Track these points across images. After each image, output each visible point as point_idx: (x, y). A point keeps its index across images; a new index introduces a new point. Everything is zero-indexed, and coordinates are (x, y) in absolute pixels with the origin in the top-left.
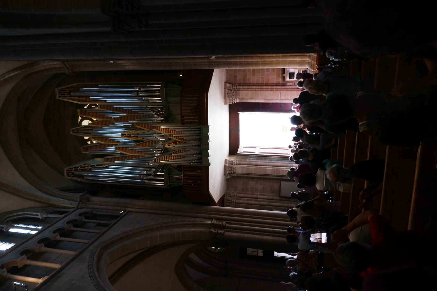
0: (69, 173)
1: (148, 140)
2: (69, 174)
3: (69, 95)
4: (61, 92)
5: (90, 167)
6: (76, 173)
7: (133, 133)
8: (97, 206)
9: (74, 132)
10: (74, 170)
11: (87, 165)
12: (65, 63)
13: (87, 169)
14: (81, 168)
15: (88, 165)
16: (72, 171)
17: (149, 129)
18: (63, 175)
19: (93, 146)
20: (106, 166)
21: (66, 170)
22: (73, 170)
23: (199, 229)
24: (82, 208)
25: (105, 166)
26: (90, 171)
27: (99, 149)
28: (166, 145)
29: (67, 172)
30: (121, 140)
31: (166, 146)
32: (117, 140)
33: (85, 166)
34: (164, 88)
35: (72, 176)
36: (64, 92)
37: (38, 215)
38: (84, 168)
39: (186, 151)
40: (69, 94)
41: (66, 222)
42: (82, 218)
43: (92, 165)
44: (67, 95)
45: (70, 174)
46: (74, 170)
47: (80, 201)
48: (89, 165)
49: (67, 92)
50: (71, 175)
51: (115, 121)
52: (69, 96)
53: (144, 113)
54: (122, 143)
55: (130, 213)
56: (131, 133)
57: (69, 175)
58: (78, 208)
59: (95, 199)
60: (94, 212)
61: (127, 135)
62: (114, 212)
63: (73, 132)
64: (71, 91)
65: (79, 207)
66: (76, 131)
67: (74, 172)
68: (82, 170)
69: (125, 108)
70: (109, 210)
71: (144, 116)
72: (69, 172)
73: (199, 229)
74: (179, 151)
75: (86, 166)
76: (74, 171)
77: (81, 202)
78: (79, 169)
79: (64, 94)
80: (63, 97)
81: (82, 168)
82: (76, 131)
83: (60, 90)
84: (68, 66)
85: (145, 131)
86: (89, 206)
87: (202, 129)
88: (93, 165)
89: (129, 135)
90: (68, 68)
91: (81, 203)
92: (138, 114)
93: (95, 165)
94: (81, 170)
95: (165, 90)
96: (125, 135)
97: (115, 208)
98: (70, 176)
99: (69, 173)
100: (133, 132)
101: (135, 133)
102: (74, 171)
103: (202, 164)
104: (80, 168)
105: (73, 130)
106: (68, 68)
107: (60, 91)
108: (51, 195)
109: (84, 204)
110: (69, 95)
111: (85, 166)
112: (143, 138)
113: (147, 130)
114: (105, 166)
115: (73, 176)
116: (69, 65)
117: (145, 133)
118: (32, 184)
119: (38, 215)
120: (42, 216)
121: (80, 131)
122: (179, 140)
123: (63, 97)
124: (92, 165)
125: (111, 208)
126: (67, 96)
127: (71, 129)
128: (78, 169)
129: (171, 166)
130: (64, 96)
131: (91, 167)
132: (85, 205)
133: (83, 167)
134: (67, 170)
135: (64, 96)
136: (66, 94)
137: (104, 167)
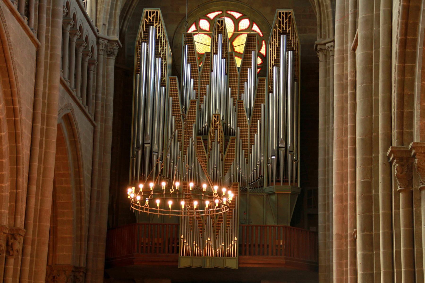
0: (152, 16)
5: (162, 53)
10: (157, 25)
25: (164, 81)
34: (290, 192)
38: (161, 42)
46: (157, 25)
72: (153, 17)
85: (222, 153)
95: (288, 194)
102: (155, 25)
111: (163, 45)
114: (164, 81)
134: (157, 13)
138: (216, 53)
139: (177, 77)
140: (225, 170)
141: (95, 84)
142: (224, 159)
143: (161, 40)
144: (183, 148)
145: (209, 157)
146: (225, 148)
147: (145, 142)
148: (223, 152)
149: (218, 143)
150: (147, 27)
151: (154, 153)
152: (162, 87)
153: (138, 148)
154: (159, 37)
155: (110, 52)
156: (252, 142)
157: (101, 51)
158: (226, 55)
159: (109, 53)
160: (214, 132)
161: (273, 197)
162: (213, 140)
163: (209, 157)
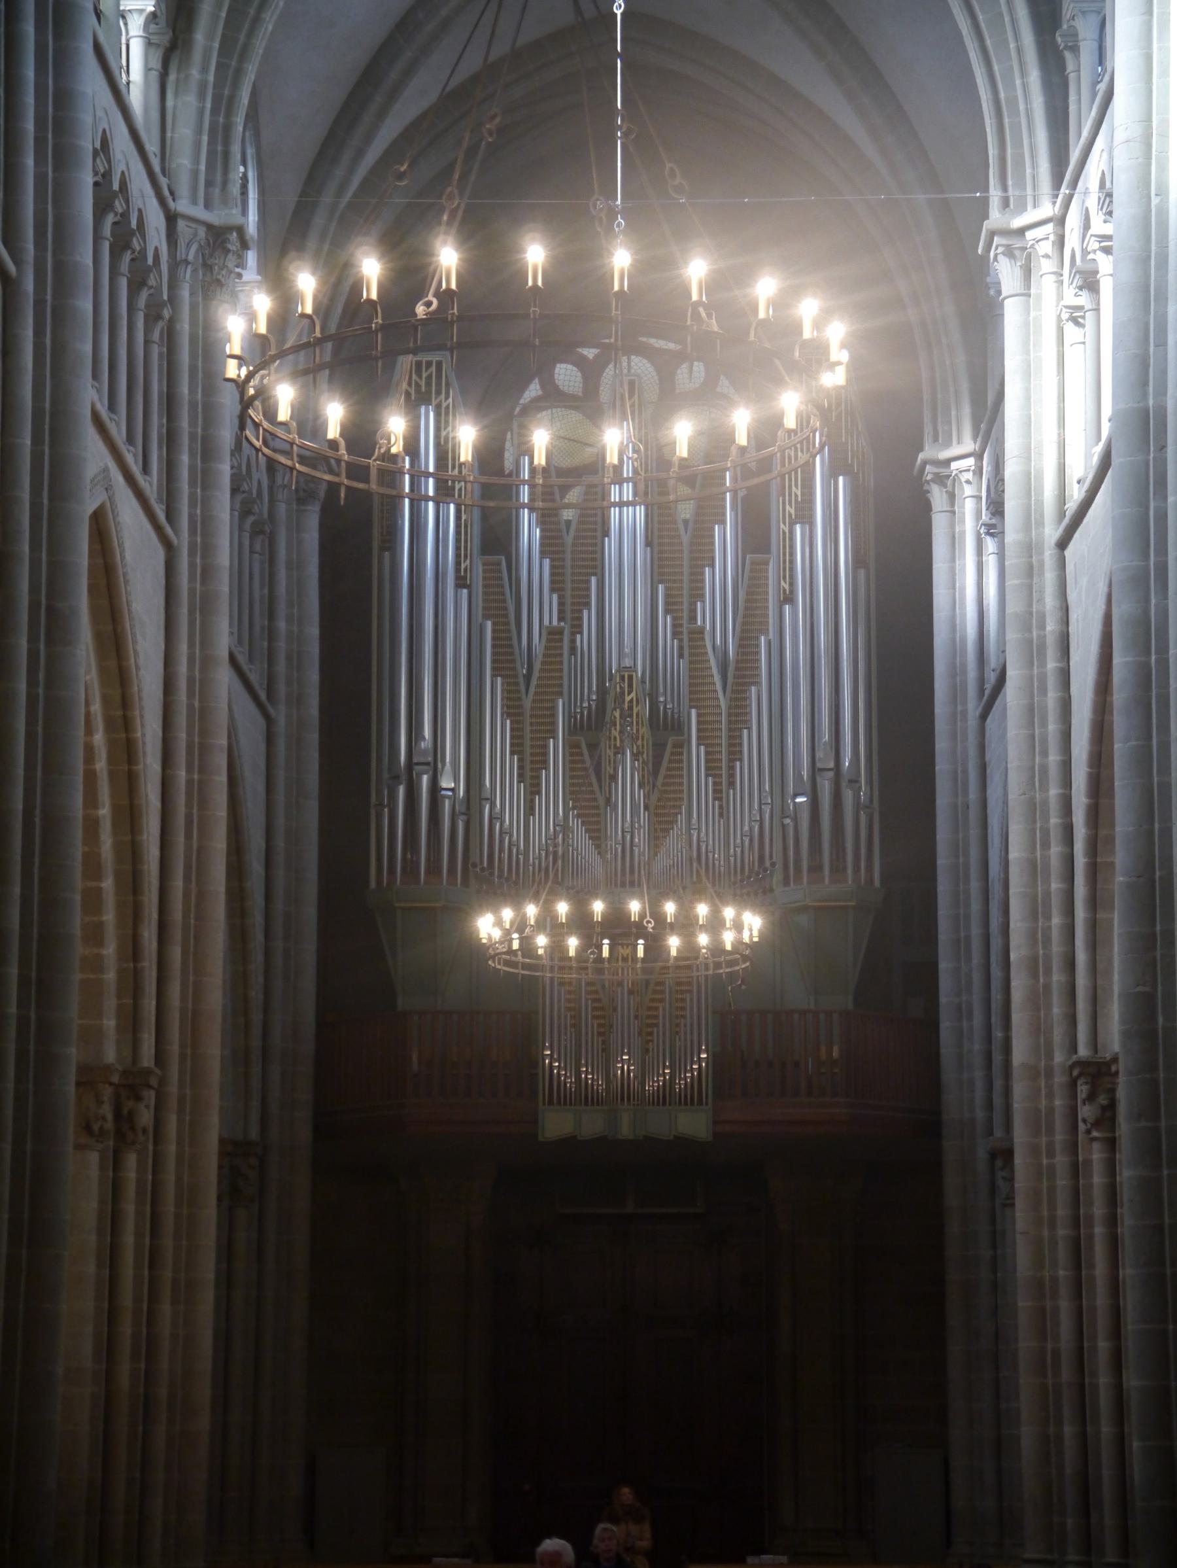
0: (424, 375)
17: (657, 807)
22: (443, 396)
25: (466, 570)
29: (429, 364)
34: (853, 904)
39: (599, 1034)
45: (423, 383)
71: (721, 783)
74: (599, 1000)
85: (647, 788)
86: (282, 508)
89: (631, 708)
92: (730, 753)
97: (282, 645)
100: (644, 729)
112: (614, 778)
125: (282, 625)
134: (439, 365)
139: (503, 558)
141: (266, 591)
147: (415, 760)
148: (648, 783)
151: (443, 792)
152: (459, 590)
153: (396, 778)
155: (305, 491)
156: (735, 753)
157: (281, 490)
159: (302, 494)
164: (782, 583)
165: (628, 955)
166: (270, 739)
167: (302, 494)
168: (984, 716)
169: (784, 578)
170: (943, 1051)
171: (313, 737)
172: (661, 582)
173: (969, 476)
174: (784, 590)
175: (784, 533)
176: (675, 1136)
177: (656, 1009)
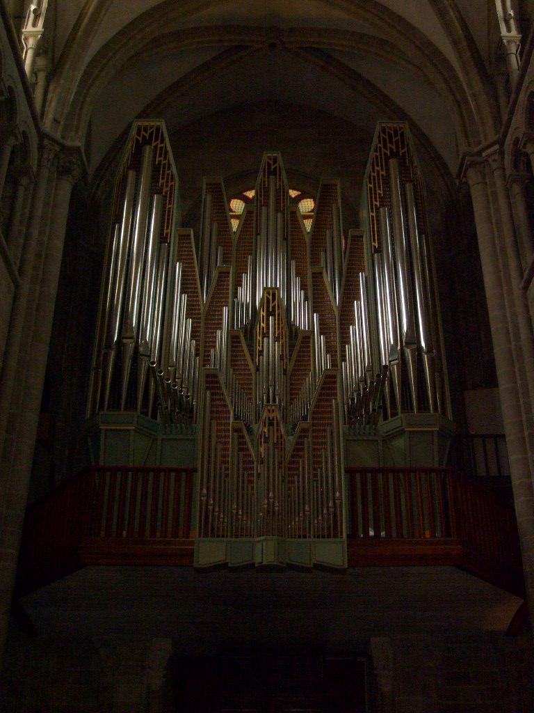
0: (149, 131)
1: (252, 367)
2: (146, 133)
3: (389, 154)
4: (396, 136)
6: (148, 150)
7: (279, 324)
8: (42, 192)
9: (271, 162)
11: (170, 184)
12: (497, 147)
13: (161, 181)
14: (165, 164)
15: (172, 186)
16: (155, 141)
18: (139, 117)
19: (222, 214)
20: (167, 238)
21: (158, 124)
22: (159, 141)
23: (438, 309)
24: (41, 147)
25: (167, 234)
26: (154, 189)
27: (215, 225)
28: (273, 411)
30: (244, 294)
31: (269, 411)
32: (247, 279)
33: (168, 179)
35: (140, 139)
36: (397, 141)
37: (34, 25)
38: (163, 175)
40: (394, 155)
41: (12, 85)
42: (16, 137)
43: (170, 197)
44: (391, 150)
45: (147, 136)
47: (63, 147)
48: (171, 189)
49: (398, 152)
50: (144, 137)
51: (313, 273)
52: (388, 153)
53: (345, 360)
54: (237, 293)
55: (13, 289)
56: (279, 319)
57: (143, 133)
58: (42, 136)
59: (65, 190)
60: (24, 181)
61: (271, 305)
62: (22, 241)
63: (270, 159)
64: (402, 160)
65: (46, 142)
66: (273, 167)
67: (150, 144)
68: (156, 169)
69: (360, 307)
70: (29, 226)
72: (151, 134)
73: (438, 309)
75: (167, 182)
76: (154, 144)
77: (61, 150)
78: (160, 161)
79: (391, 142)
80: (384, 139)
81: (164, 171)
82: (273, 167)
83: (402, 134)
84: (484, 154)
86: (45, 172)
87: (330, 540)
88: (170, 201)
90: (480, 153)
91: (57, 148)
93: (171, 206)
94: (157, 163)
95: (432, 432)
96: (271, 298)
98: (139, 133)
99: (149, 131)
101: (279, 329)
102: (154, 144)
103: (200, 536)
104: (163, 162)
105: (275, 162)
106: (480, 153)
107: (399, 133)
108: (87, 74)
109: (52, 156)
110: (389, 154)
111: (168, 179)
112: (261, 352)
113: (290, 367)
114: (167, 234)
115: (137, 140)
116: (489, 156)
117: (258, 373)
118: (121, 33)
119: (34, 25)
120: (33, 35)
121: (272, 177)
122: (288, 458)
123: (385, 140)
124: (170, 197)
125: (35, 232)
126: (385, 147)
127: (280, 155)
128: (162, 158)
129: (163, 440)
130: (388, 142)
131: (166, 197)
132: (49, 160)
133: (167, 172)
134: (158, 129)
135: (388, 142)
136: (394, 147)
137: (165, 232)
138: (267, 205)
140: (291, 394)
141: (27, 211)
142: (289, 373)
143: (164, 171)
144: (201, 351)
145: (258, 369)
146: (291, 355)
149: (276, 339)
150: (139, 148)
154: (160, 161)
155: (63, 167)
156: (345, 340)
158: (284, 210)
160: (268, 320)
161: (400, 443)
162: (266, 335)
163: (258, 369)
164: (373, 244)
165: (273, 418)
166: (16, 298)
167: (60, 169)
168: (526, 288)
169: (374, 240)
170: (520, 519)
171: (50, 306)
172: (292, 258)
173: (496, 157)
174: (375, 247)
175: (373, 217)
176: (314, 563)
177: (298, 462)
